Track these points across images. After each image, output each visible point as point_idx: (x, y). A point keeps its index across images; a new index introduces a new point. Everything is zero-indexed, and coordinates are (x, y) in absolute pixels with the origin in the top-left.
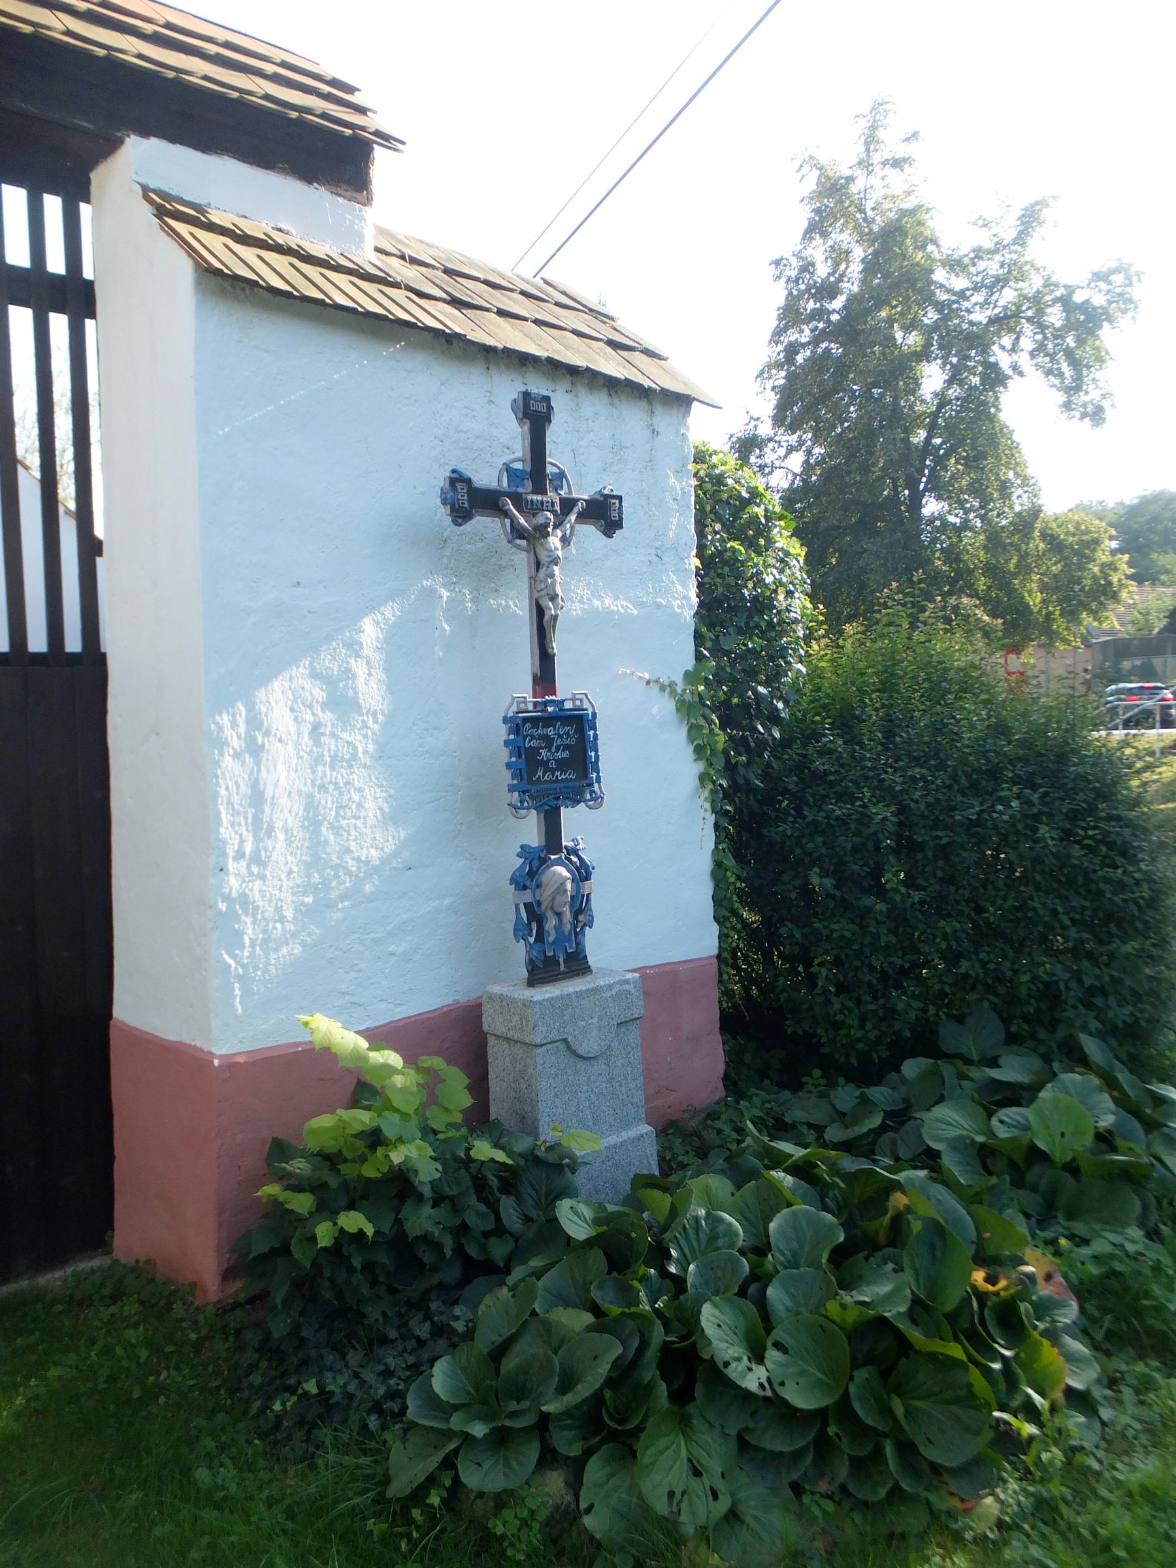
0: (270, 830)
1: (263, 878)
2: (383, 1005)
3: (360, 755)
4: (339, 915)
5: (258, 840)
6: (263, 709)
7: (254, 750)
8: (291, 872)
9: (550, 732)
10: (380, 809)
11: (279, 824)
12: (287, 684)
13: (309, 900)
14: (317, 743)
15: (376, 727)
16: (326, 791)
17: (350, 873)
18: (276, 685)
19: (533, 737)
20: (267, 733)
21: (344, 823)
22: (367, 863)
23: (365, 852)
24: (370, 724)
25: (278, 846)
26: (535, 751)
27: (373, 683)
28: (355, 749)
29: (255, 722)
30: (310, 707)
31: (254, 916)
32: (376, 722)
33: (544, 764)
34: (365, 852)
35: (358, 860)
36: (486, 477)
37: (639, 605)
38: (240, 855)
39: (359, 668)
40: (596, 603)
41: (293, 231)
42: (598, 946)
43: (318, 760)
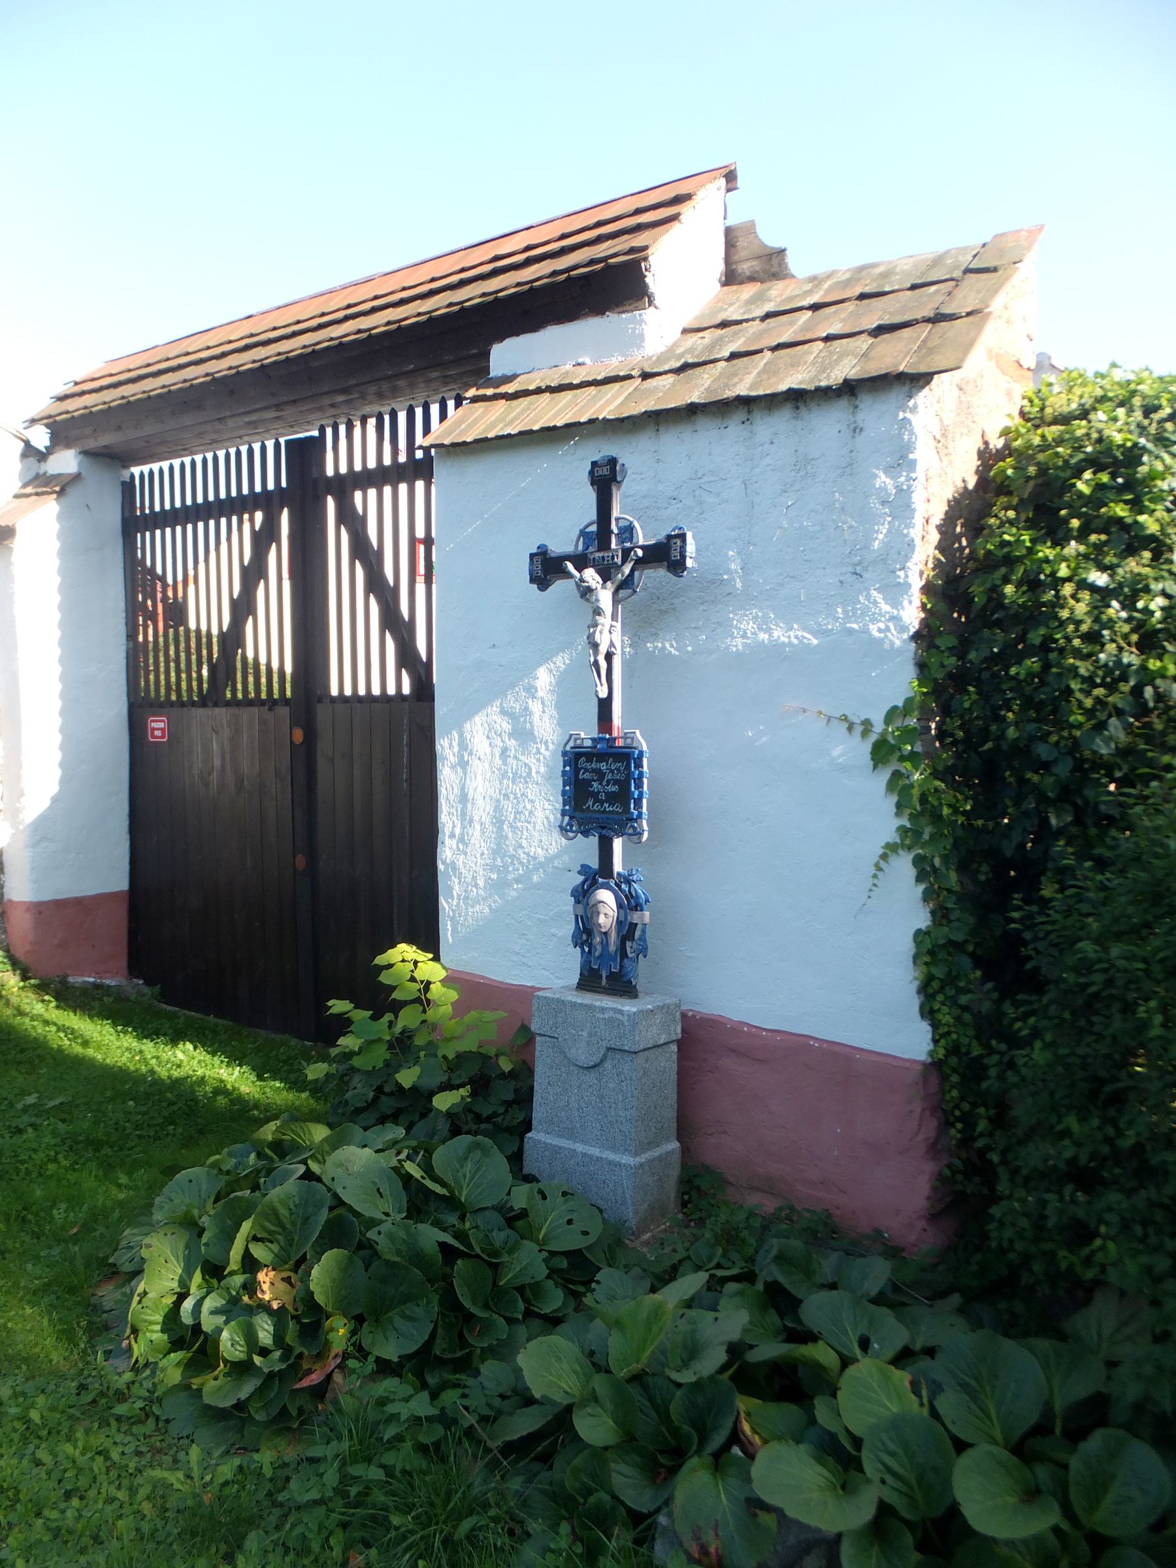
0: (471, 821)
1: (466, 854)
2: (546, 973)
3: (533, 774)
4: (515, 894)
5: (463, 827)
6: (468, 737)
7: (463, 764)
8: (483, 854)
9: (603, 766)
10: (547, 818)
11: (476, 818)
12: (484, 718)
13: (495, 876)
14: (505, 763)
15: (547, 754)
16: (508, 799)
17: (522, 864)
18: (477, 719)
19: (586, 770)
20: (471, 754)
21: (519, 824)
22: (535, 858)
23: (533, 849)
24: (543, 750)
25: (476, 832)
26: (588, 783)
27: (546, 718)
28: (530, 769)
29: (463, 745)
30: (500, 735)
31: (460, 878)
32: (547, 749)
33: (595, 795)
34: (533, 849)
35: (528, 855)
36: (563, 543)
37: (819, 632)
38: (452, 836)
39: (535, 707)
40: (762, 636)
41: (588, 361)
42: (642, 972)
43: (504, 775)
